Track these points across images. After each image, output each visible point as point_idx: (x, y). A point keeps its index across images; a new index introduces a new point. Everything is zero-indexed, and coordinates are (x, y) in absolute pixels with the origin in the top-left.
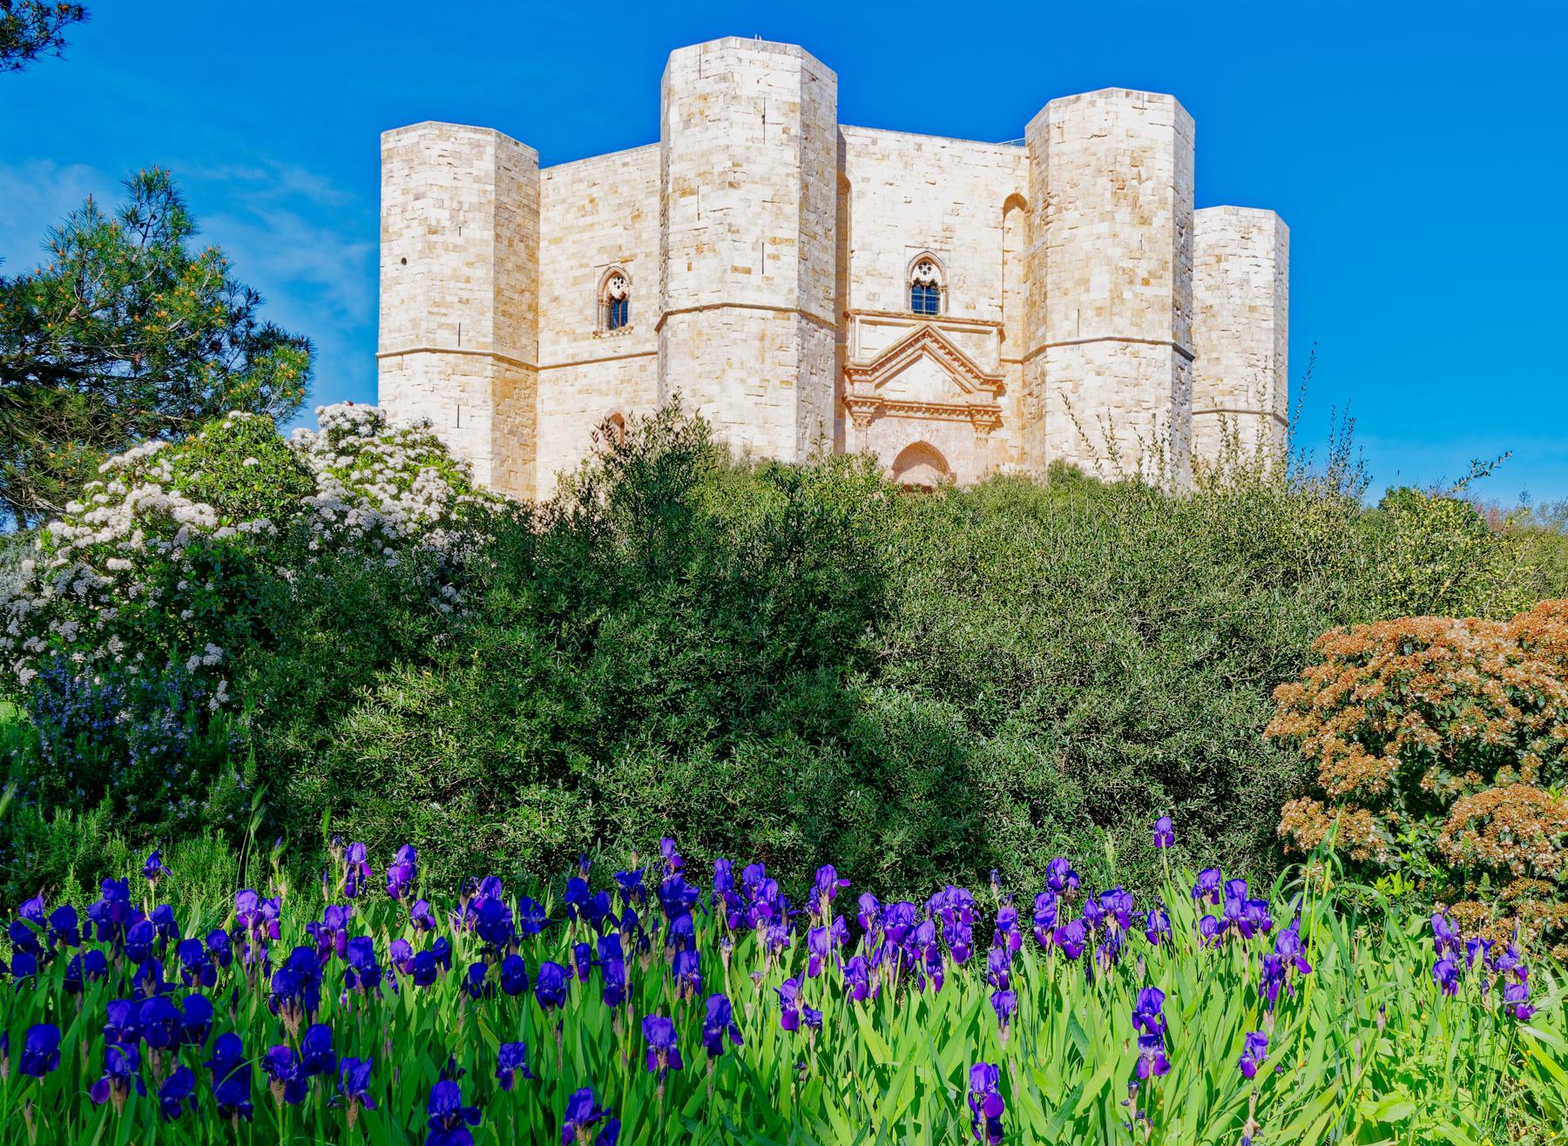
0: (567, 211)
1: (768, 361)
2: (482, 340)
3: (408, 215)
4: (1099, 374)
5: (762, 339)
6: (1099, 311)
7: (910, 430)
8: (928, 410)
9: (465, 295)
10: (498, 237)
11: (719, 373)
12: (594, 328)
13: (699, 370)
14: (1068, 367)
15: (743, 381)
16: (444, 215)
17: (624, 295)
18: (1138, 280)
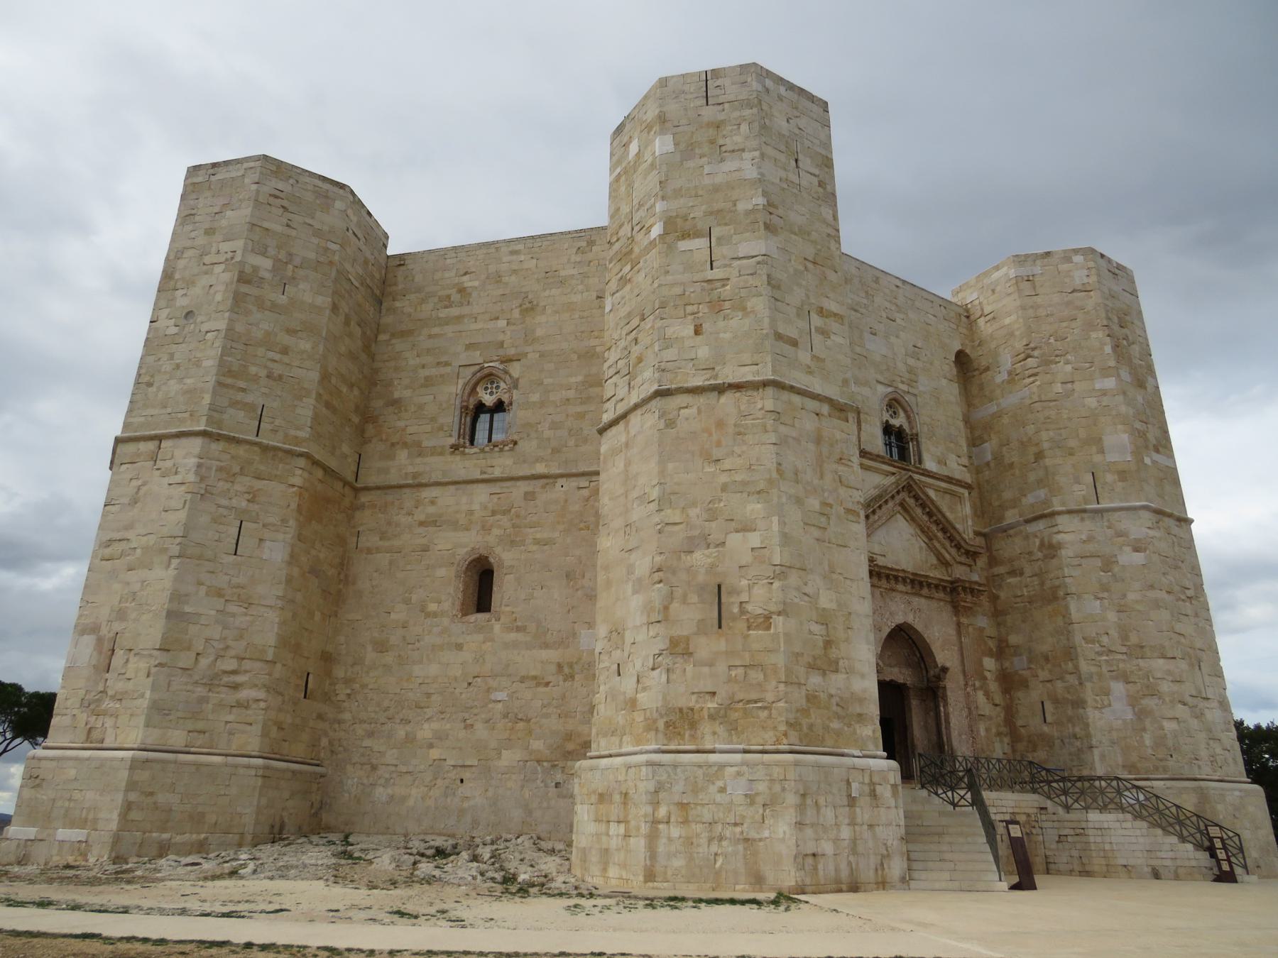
0: (423, 301)
1: (829, 477)
2: (292, 432)
3: (207, 259)
4: (1136, 550)
5: (818, 440)
6: (1123, 475)
8: (912, 581)
9: (278, 369)
10: (335, 308)
11: (762, 485)
12: (452, 441)
13: (724, 478)
14: (1091, 539)
15: (799, 501)
16: (266, 264)
17: (500, 407)
18: (1151, 446)
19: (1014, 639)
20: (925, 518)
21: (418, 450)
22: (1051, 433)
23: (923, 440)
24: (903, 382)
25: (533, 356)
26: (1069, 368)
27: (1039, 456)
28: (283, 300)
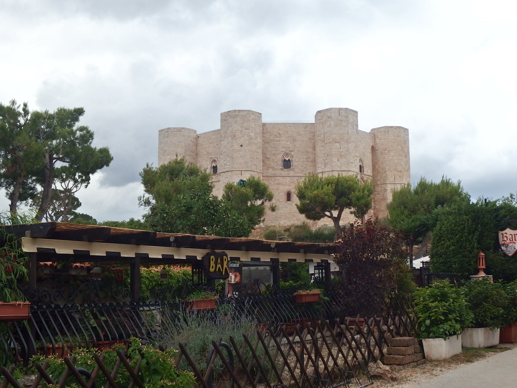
0: (271, 135)
19: (377, 207)
21: (273, 169)
25: (296, 151)
26: (393, 154)
27: (385, 172)
28: (256, 142)
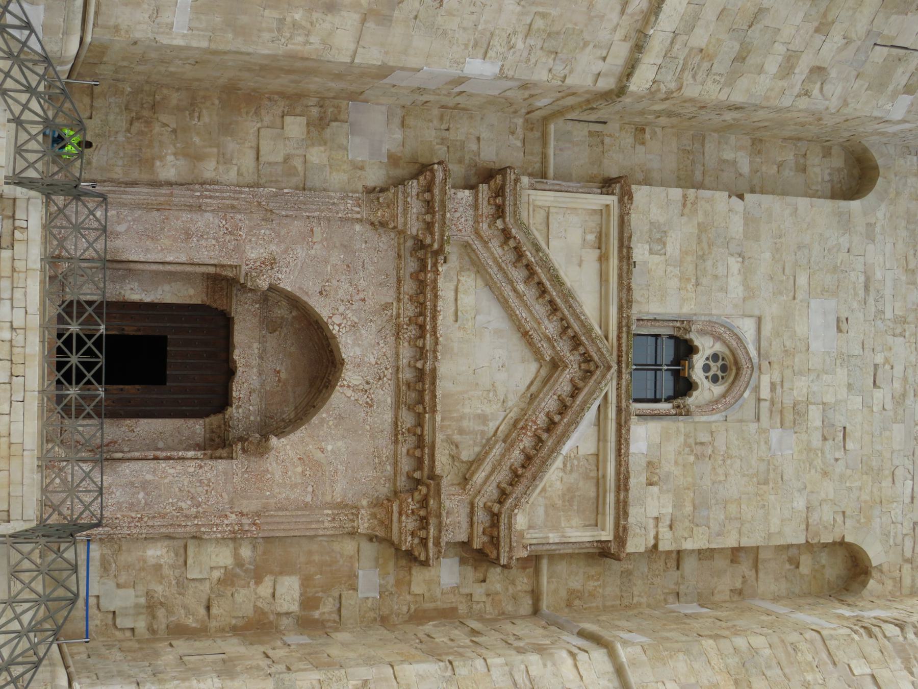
7: (368, 333)
8: (420, 374)
20: (542, 420)
22: (767, 652)
23: (681, 425)
24: (773, 386)
